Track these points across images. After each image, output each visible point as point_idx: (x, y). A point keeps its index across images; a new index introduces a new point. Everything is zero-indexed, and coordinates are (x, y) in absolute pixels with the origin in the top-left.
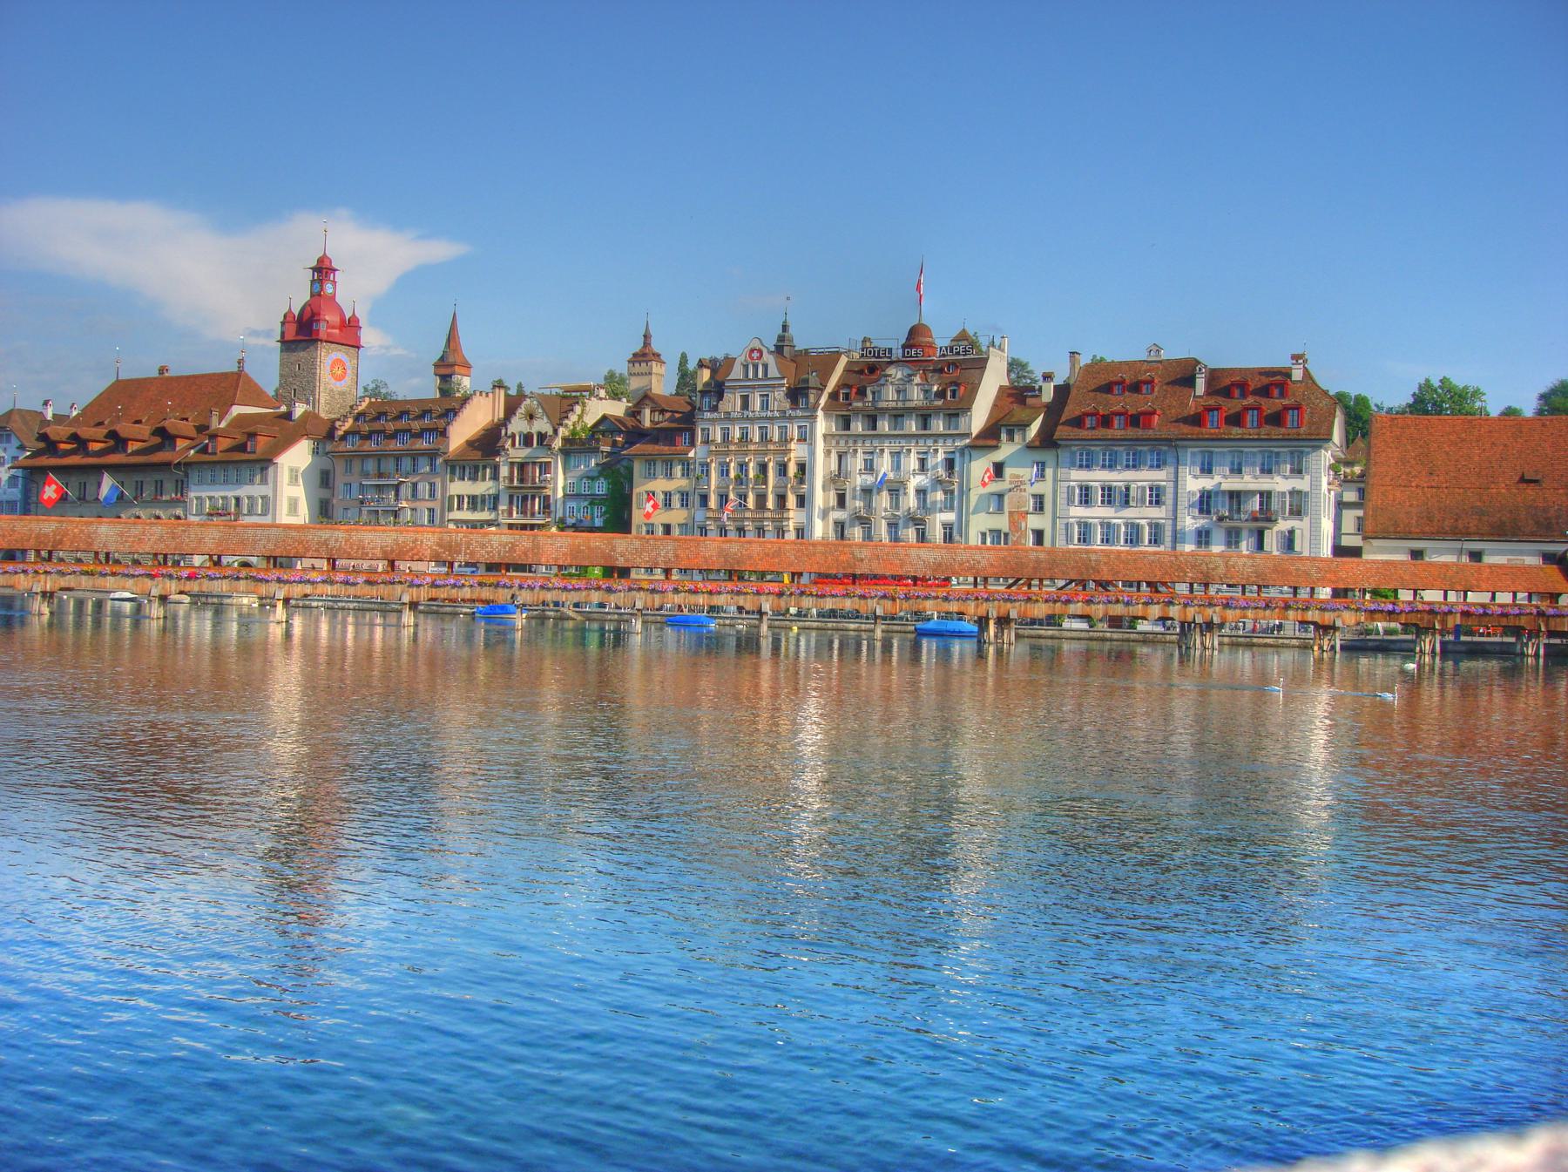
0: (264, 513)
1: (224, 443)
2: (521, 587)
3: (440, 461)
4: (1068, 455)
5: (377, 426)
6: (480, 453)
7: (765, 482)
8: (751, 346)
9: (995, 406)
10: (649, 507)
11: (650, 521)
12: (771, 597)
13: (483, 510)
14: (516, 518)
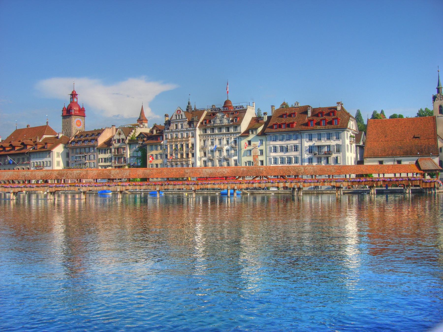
0: (50, 166)
1: (39, 146)
2: (82, 186)
3: (96, 148)
4: (269, 137)
5: (86, 138)
6: (107, 145)
7: (183, 150)
8: (178, 109)
9: (250, 123)
10: (151, 159)
11: (152, 163)
12: (159, 186)
13: (108, 162)
14: (117, 164)
